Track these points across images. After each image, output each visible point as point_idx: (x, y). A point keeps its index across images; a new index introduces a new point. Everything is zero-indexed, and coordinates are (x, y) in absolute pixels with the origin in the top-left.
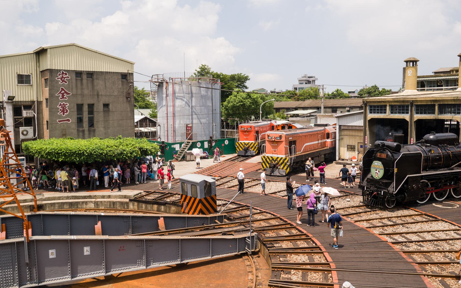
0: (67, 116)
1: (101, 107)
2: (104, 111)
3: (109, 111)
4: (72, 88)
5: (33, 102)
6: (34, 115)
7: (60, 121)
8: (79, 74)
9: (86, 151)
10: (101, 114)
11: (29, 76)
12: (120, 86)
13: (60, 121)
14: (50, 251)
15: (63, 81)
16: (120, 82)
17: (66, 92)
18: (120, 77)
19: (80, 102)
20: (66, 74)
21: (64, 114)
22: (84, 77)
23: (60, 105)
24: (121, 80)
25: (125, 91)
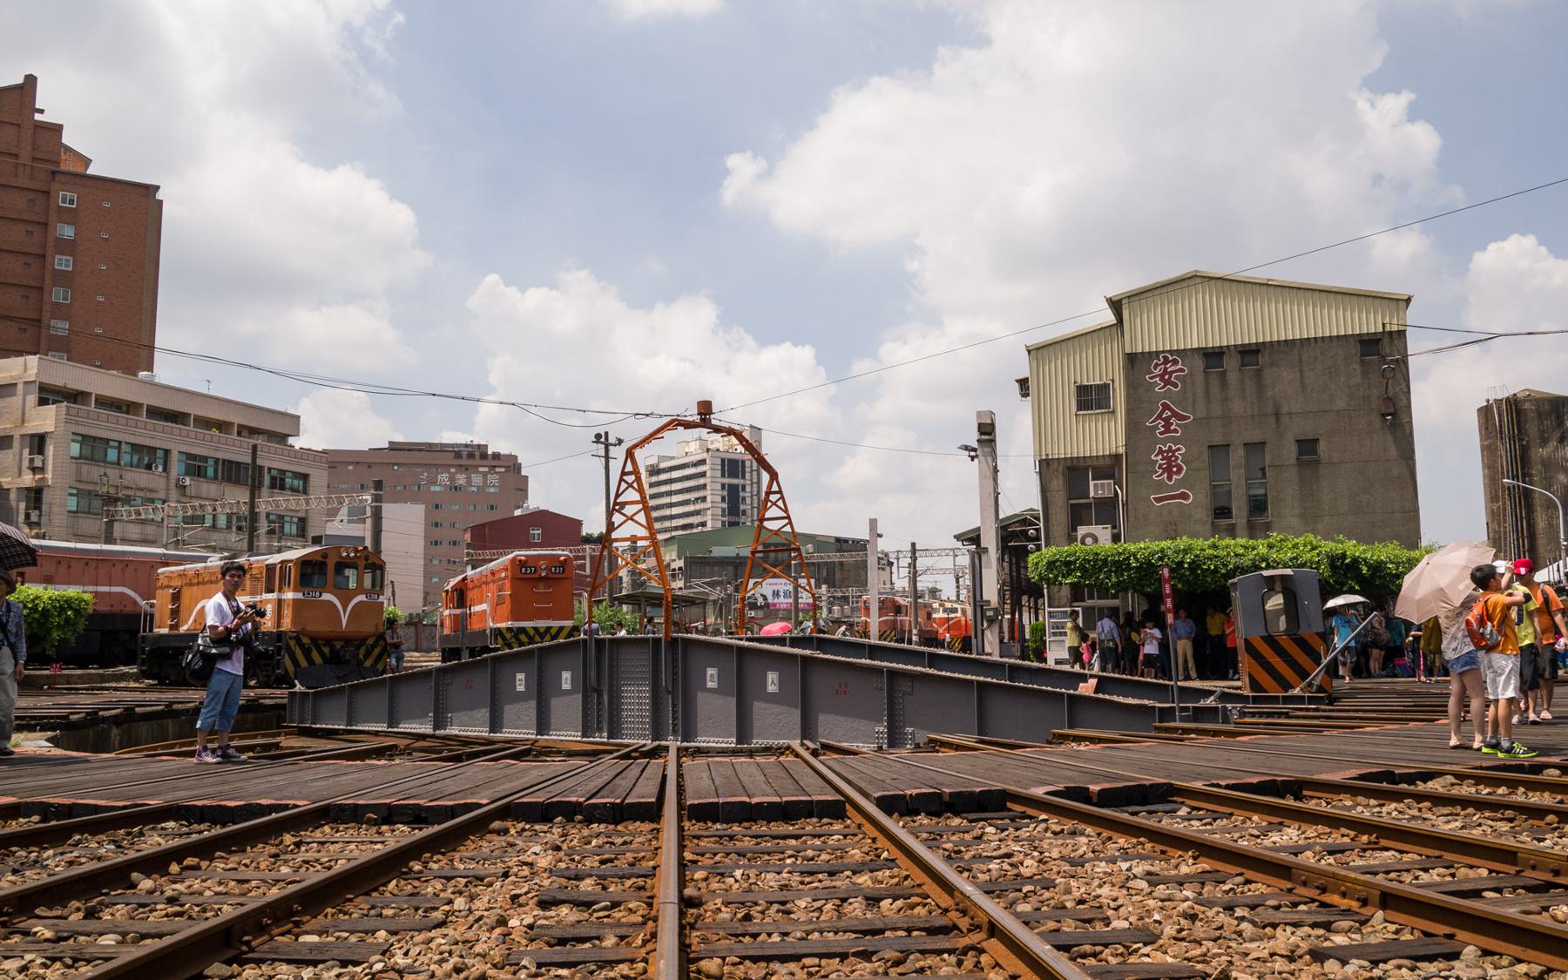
0: (1180, 484)
1: (1290, 452)
2: (1300, 463)
3: (1317, 462)
4: (1194, 401)
5: (1117, 457)
6: (1116, 494)
7: (1158, 500)
8: (1212, 356)
9: (1135, 555)
10: (1291, 474)
11: (1106, 386)
12: (1357, 379)
13: (1158, 500)
14: (711, 671)
15: (1167, 382)
16: (1357, 366)
17: (1175, 414)
18: (1355, 349)
19: (1218, 439)
20: (1175, 362)
21: (1170, 478)
22: (1231, 363)
23: (1161, 452)
24: (1357, 358)
25: (1376, 392)
